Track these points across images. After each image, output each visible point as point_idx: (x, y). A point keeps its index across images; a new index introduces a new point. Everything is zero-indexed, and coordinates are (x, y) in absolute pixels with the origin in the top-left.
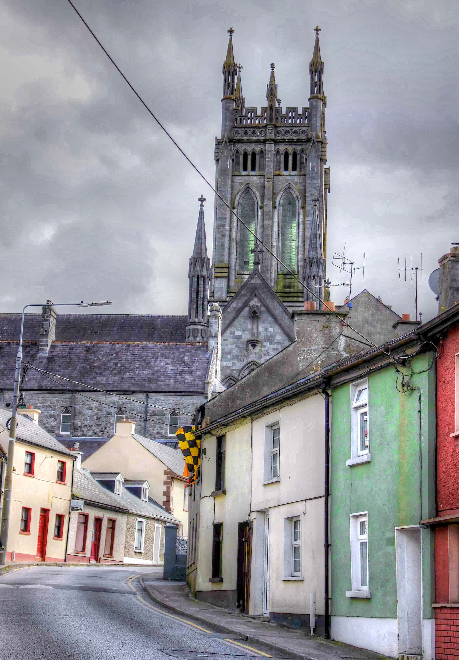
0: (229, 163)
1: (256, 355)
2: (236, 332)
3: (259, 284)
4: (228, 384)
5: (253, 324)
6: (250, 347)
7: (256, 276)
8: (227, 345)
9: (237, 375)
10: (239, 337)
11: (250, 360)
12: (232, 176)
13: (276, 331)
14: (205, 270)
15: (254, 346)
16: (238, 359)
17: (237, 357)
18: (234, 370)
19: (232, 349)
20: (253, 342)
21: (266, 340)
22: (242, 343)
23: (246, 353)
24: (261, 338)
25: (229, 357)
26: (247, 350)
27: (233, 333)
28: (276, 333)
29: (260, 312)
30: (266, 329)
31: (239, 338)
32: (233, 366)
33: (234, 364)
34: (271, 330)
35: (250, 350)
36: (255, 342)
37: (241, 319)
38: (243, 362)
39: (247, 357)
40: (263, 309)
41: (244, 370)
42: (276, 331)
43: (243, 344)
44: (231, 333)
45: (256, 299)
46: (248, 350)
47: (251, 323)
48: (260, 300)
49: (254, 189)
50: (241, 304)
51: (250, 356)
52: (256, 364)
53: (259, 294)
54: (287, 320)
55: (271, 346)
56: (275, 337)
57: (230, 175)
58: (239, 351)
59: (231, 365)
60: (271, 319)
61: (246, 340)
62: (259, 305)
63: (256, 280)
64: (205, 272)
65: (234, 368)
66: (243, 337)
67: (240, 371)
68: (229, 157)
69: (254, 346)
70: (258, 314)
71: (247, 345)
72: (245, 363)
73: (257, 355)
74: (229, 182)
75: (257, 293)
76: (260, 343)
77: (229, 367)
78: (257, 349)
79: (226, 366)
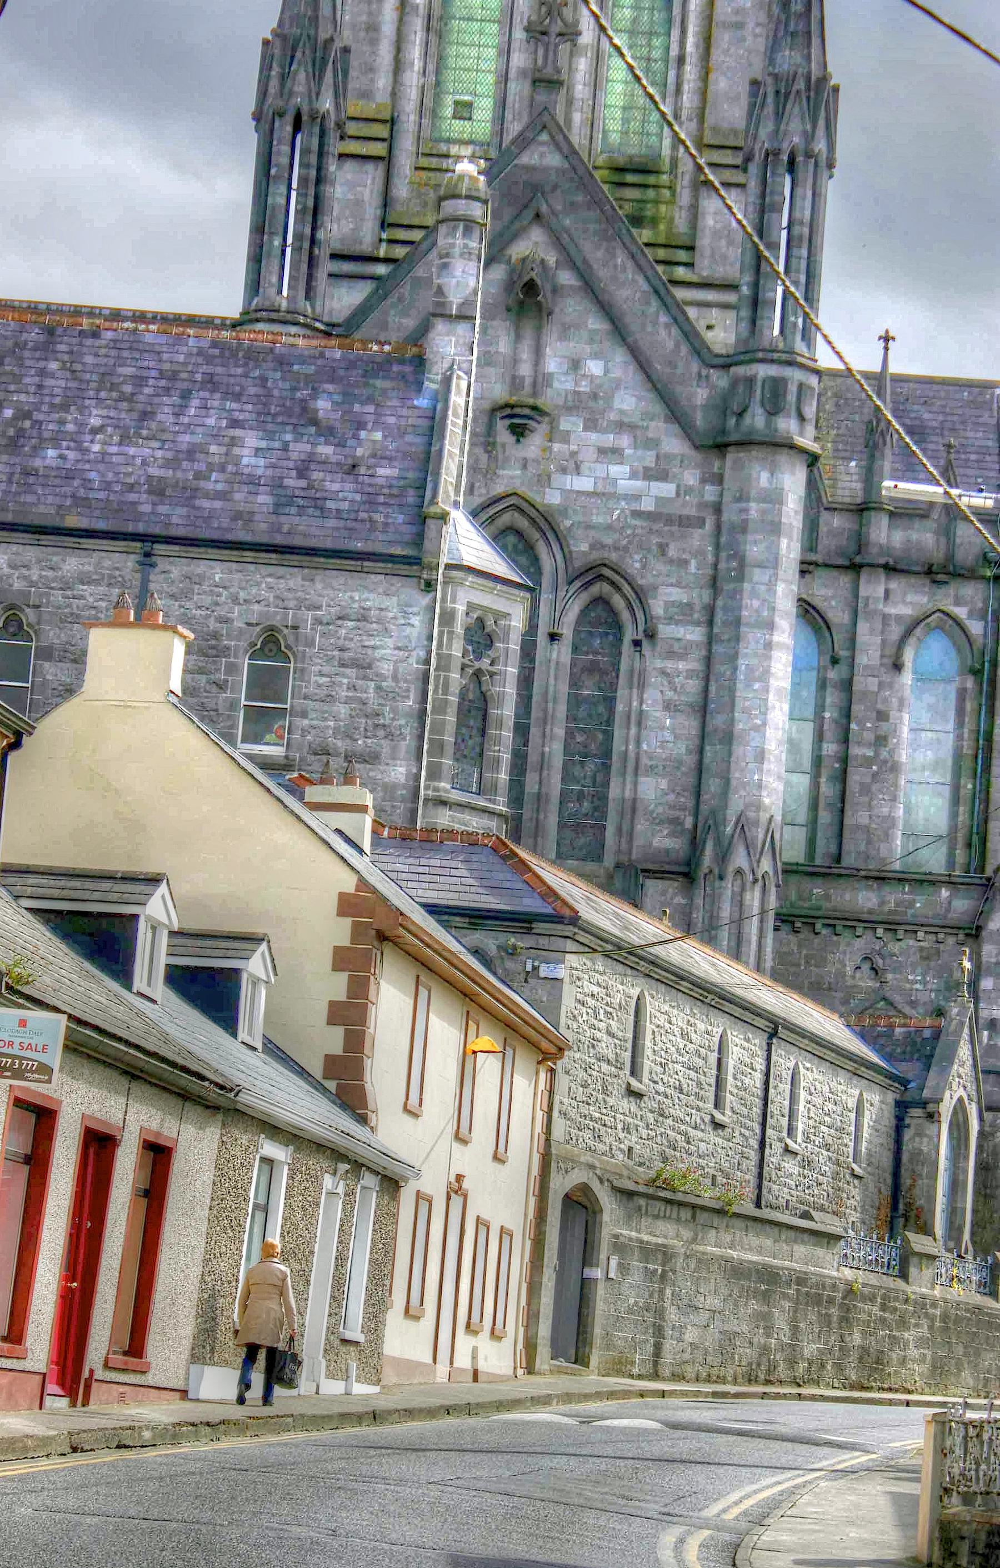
1: (525, 467)
3: (557, 170)
5: (518, 337)
6: (503, 435)
7: (544, 137)
11: (499, 489)
13: (616, 373)
15: (519, 432)
20: (518, 411)
21: (570, 409)
24: (547, 400)
28: (618, 384)
29: (555, 290)
30: (575, 365)
34: (595, 367)
35: (504, 446)
36: (527, 411)
40: (566, 278)
42: (616, 373)
46: (494, 444)
47: (513, 334)
48: (557, 241)
51: (501, 472)
52: (525, 506)
53: (554, 213)
54: (663, 333)
55: (593, 437)
56: (609, 398)
60: (596, 323)
62: (551, 259)
63: (542, 155)
64: (327, 104)
69: (519, 432)
71: (490, 428)
73: (532, 470)
75: (544, 209)
76: (547, 419)
78: (533, 445)
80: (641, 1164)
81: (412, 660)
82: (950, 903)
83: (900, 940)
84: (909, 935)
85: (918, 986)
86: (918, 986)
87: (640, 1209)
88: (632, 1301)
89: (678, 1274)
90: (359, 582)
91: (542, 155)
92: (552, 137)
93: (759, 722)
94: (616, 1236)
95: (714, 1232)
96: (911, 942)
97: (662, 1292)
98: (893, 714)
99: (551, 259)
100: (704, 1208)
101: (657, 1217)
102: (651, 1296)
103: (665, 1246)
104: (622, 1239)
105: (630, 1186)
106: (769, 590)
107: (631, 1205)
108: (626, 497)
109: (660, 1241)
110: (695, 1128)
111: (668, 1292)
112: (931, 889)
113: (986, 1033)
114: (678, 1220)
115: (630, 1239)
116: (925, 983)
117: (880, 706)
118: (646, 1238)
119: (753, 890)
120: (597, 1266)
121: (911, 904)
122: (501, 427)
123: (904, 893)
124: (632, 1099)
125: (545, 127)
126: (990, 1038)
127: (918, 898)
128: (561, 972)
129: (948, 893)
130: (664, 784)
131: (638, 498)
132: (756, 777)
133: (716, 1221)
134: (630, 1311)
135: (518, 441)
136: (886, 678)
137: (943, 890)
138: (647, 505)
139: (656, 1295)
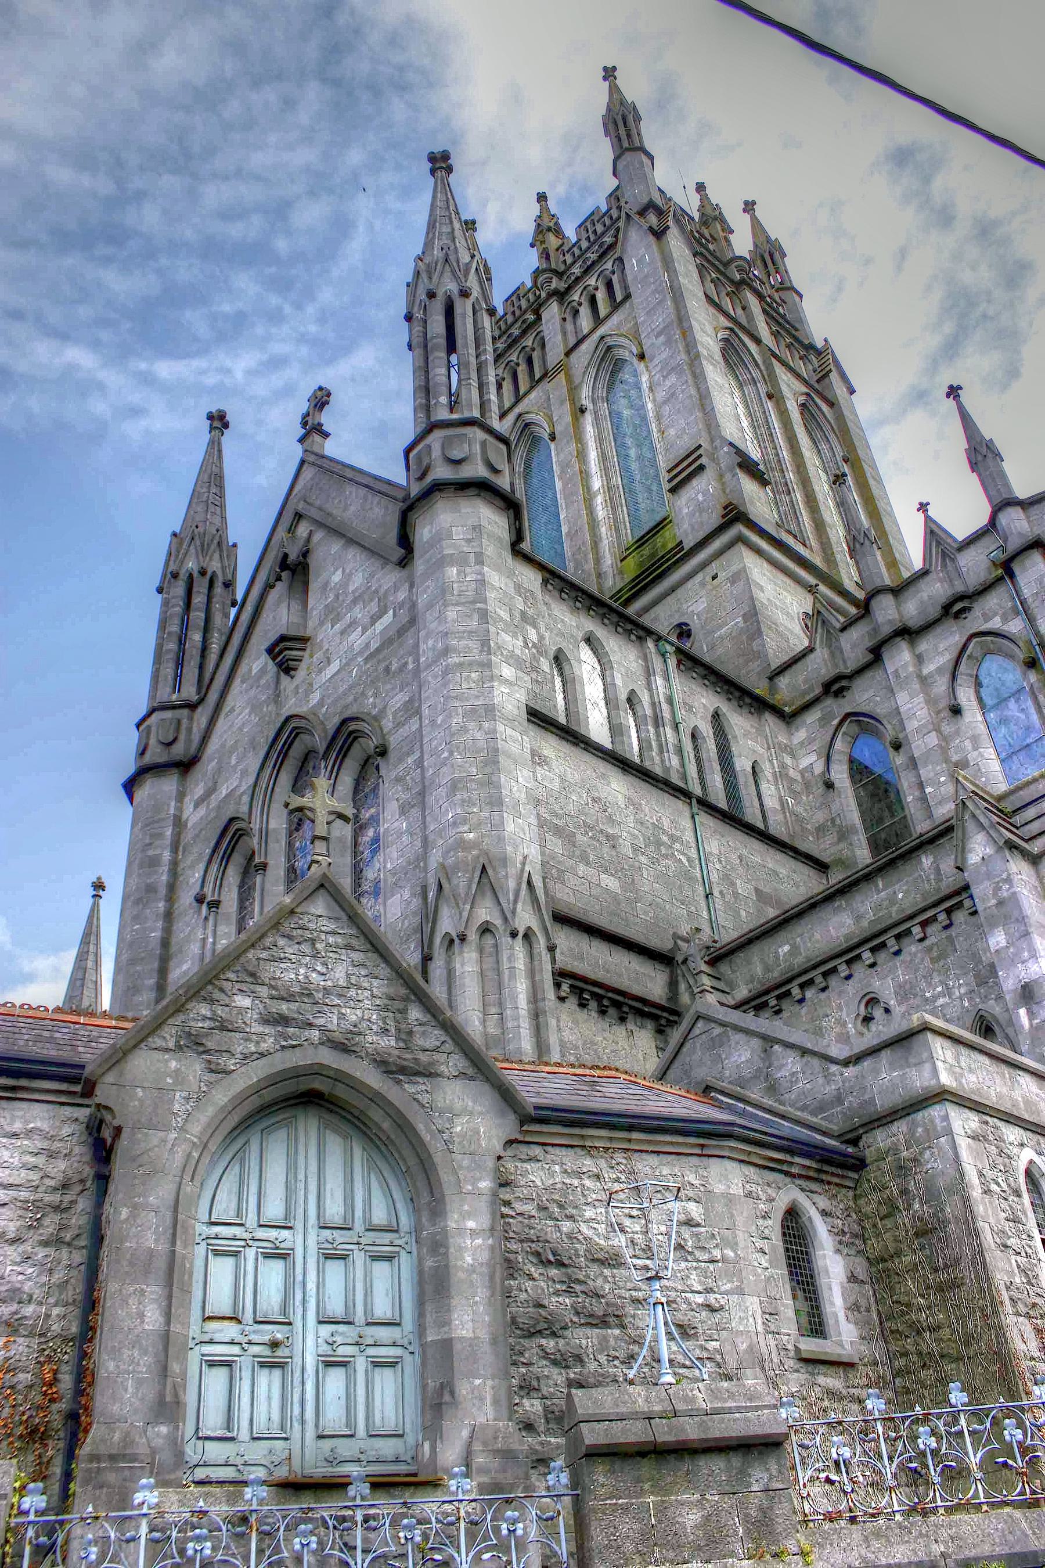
6: (285, 680)
7: (306, 465)
60: (336, 546)
82: (938, 870)
83: (897, 953)
84: (906, 941)
85: (941, 1001)
86: (941, 1001)
93: (446, 754)
96: (913, 948)
98: (972, 756)
106: (440, 623)
108: (361, 653)
112: (908, 867)
113: (1022, 1012)
116: (948, 991)
117: (955, 758)
119: (461, 952)
121: (892, 900)
123: (879, 892)
126: (1031, 1015)
127: (897, 887)
129: (931, 859)
130: (406, 894)
131: (368, 644)
132: (450, 815)
135: (292, 678)
136: (947, 729)
137: (924, 860)
138: (374, 645)
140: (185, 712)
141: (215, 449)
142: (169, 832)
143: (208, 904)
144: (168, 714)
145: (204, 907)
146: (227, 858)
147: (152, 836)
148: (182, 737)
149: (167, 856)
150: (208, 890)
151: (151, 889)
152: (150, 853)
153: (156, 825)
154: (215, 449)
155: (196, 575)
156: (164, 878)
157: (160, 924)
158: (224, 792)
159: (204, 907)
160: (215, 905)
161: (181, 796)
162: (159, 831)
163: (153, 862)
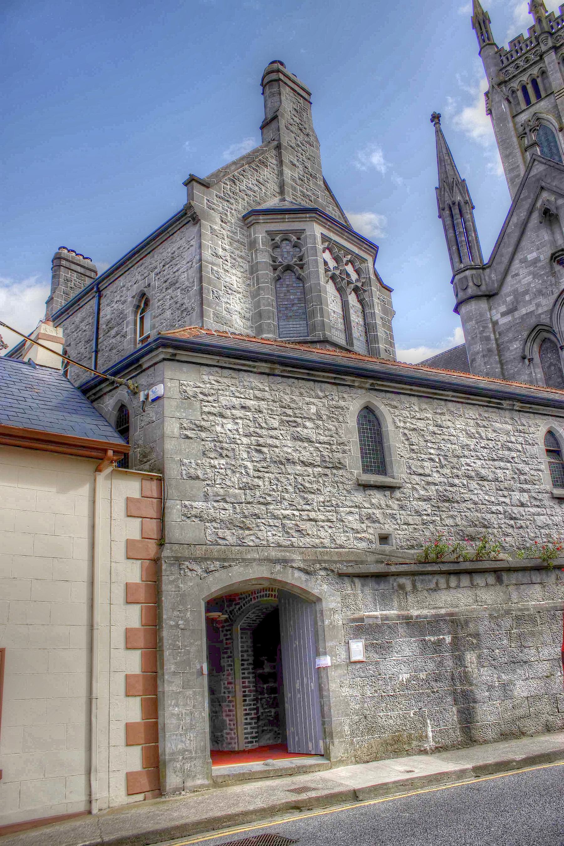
0: (504, 106)
2: (528, 256)
3: (544, 170)
4: (538, 341)
5: (553, 233)
7: (536, 163)
8: (520, 281)
9: (548, 320)
10: (536, 261)
12: (514, 117)
14: (459, 194)
16: (543, 295)
17: (540, 293)
18: (540, 314)
19: (529, 284)
20: (557, 255)
22: (543, 268)
23: (553, 279)
25: (527, 298)
26: (554, 274)
27: (524, 261)
29: (557, 208)
31: (535, 263)
32: (537, 309)
33: (538, 305)
36: (561, 253)
37: (529, 233)
38: (553, 294)
39: (557, 283)
41: (557, 306)
43: (545, 268)
44: (521, 262)
45: (545, 195)
47: (549, 232)
49: (544, 116)
50: (525, 213)
51: (561, 281)
53: (549, 184)
57: (510, 118)
58: (540, 282)
59: (534, 308)
61: (548, 260)
62: (553, 198)
63: (537, 169)
64: (459, 198)
65: (540, 311)
66: (542, 257)
67: (552, 310)
68: (502, 100)
70: (553, 211)
71: (552, 267)
72: (556, 295)
74: (511, 125)
75: (543, 184)
77: (532, 312)
79: (527, 314)
80: (412, 547)
81: (194, 264)
87: (402, 587)
88: (405, 677)
89: (482, 638)
90: (170, 242)
91: (537, 169)
92: (539, 161)
94: (361, 620)
95: (538, 587)
97: (459, 660)
99: (553, 198)
100: (510, 570)
101: (436, 589)
102: (440, 664)
103: (451, 615)
104: (366, 621)
105: (381, 568)
107: (382, 586)
109: (443, 611)
110: (522, 505)
111: (470, 657)
114: (473, 586)
115: (387, 618)
118: (415, 613)
120: (325, 654)
122: (555, 264)
124: (368, 492)
125: (534, 160)
128: (159, 389)
133: (536, 577)
134: (405, 686)
139: (449, 663)
140: (481, 271)
141: (439, 133)
142: (490, 325)
143: (529, 359)
144: (474, 272)
145: (527, 361)
146: (534, 340)
147: (484, 327)
148: (483, 282)
149: (492, 336)
150: (527, 353)
151: (490, 350)
152: (484, 334)
153: (484, 322)
154: (439, 133)
155: (462, 203)
156: (494, 346)
157: (499, 366)
158: (524, 311)
159: (527, 361)
160: (531, 360)
161: (490, 309)
162: (486, 325)
163: (488, 339)
